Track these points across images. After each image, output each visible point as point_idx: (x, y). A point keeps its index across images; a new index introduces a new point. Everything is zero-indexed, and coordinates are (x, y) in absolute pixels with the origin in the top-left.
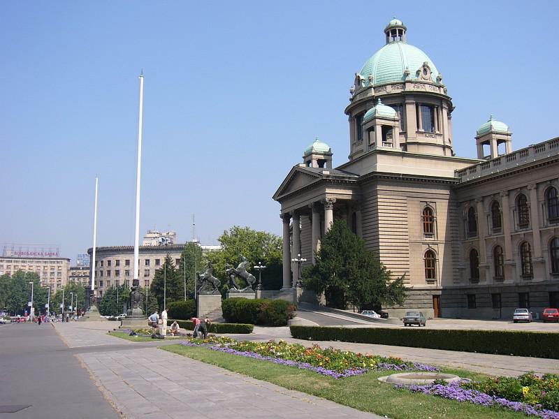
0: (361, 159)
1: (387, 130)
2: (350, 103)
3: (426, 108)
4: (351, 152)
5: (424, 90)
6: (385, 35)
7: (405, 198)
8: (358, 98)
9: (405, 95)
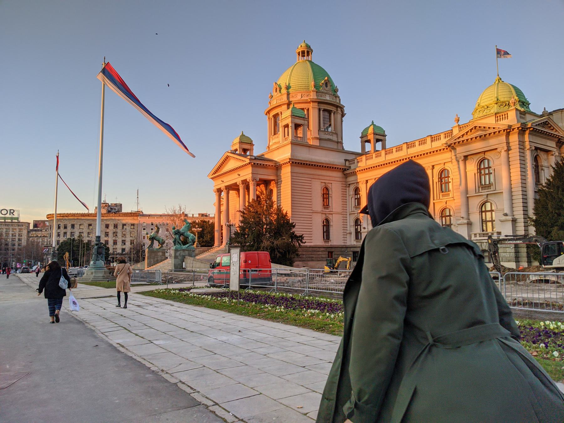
5: (324, 98)
7: (310, 179)
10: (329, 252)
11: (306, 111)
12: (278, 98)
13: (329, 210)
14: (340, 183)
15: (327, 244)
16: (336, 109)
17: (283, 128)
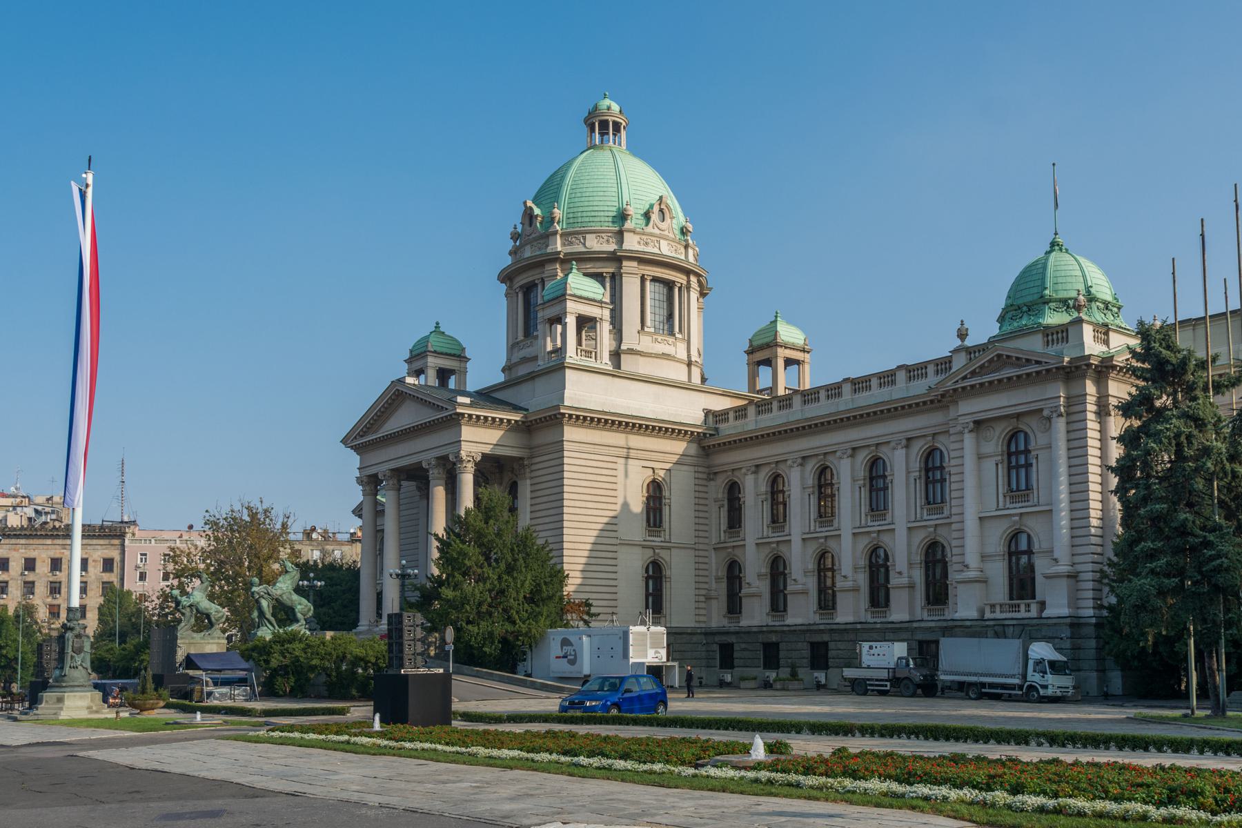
0: (532, 377)
1: (585, 323)
2: (509, 260)
3: (660, 288)
4: (509, 359)
5: (656, 251)
6: (585, 129)
7: (614, 459)
8: (528, 253)
9: (616, 258)
13: (663, 539)
14: (692, 469)
16: (685, 278)
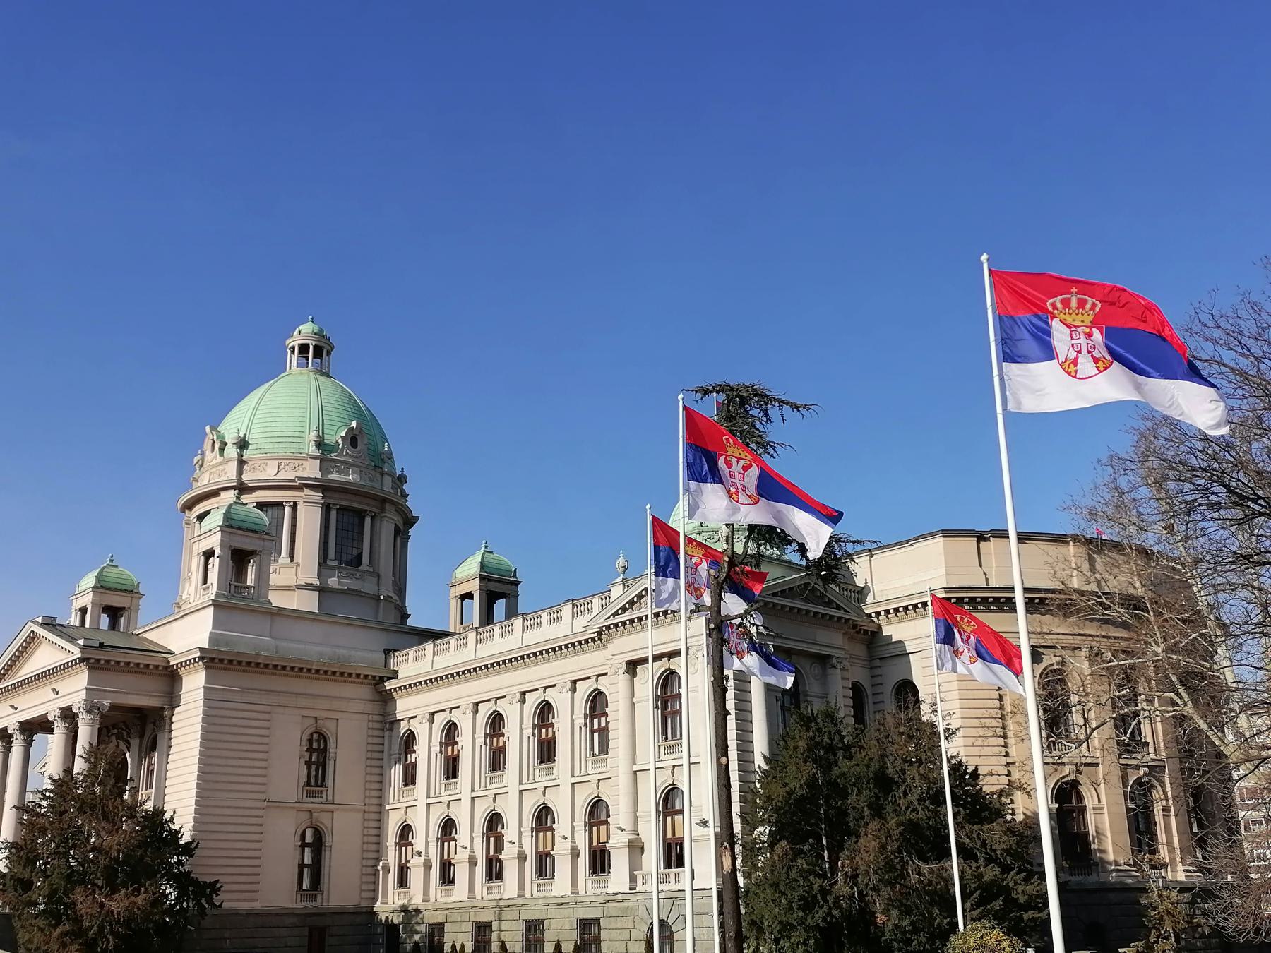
7: (268, 709)
10: (311, 929)
11: (287, 510)
12: (214, 470)
13: (324, 800)
15: (308, 904)
17: (202, 559)
